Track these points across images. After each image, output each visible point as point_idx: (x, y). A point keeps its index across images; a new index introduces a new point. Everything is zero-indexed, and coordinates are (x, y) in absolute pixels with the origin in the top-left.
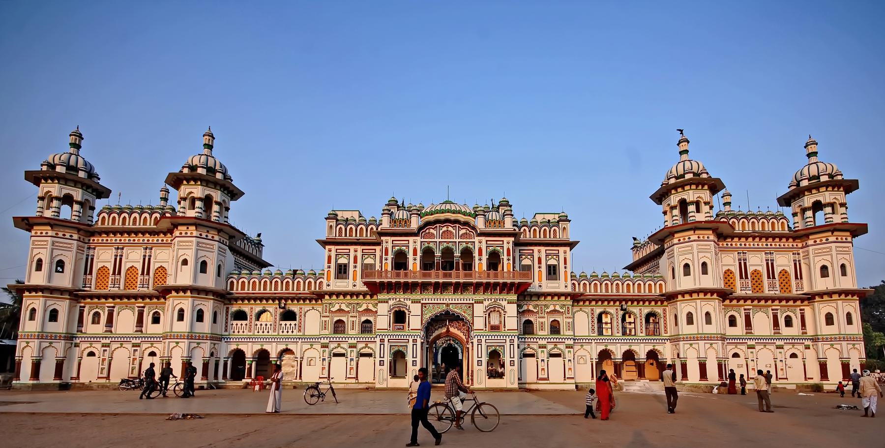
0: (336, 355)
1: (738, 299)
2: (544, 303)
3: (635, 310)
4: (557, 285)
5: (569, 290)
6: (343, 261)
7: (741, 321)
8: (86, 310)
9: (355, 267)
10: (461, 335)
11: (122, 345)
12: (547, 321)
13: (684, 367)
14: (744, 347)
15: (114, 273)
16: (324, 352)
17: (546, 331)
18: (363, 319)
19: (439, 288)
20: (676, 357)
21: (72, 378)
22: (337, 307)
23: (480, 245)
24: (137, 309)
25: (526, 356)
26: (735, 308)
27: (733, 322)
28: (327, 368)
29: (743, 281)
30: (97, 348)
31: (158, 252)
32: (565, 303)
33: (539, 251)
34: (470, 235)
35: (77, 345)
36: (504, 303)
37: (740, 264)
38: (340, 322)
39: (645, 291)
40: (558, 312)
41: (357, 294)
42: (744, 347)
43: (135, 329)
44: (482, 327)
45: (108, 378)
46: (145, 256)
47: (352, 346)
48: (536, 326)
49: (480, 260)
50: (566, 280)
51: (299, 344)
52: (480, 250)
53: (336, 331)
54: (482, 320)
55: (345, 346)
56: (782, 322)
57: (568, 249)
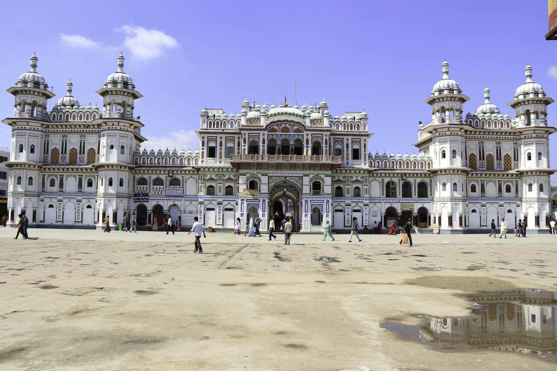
0: (209, 209)
2: (350, 175)
3: (411, 180)
6: (212, 144)
7: (478, 189)
8: (46, 177)
9: (221, 149)
10: (293, 196)
11: (70, 200)
14: (479, 205)
15: (62, 153)
16: (201, 206)
18: (227, 185)
19: (279, 166)
21: (41, 221)
22: (209, 177)
23: (307, 136)
24: (78, 177)
25: (337, 211)
27: (473, 189)
28: (203, 218)
29: (481, 161)
30: (54, 202)
31: (89, 138)
32: (364, 175)
33: (347, 139)
34: (301, 130)
35: (42, 201)
36: (323, 176)
37: (480, 149)
38: (211, 187)
40: (359, 181)
41: (222, 168)
42: (479, 205)
43: (77, 190)
44: (308, 192)
45: (63, 222)
46: (81, 141)
47: (220, 204)
48: (345, 191)
49: (307, 147)
50: (365, 160)
51: (183, 201)
52: (307, 140)
53: (208, 193)
55: (215, 203)
56: (504, 189)
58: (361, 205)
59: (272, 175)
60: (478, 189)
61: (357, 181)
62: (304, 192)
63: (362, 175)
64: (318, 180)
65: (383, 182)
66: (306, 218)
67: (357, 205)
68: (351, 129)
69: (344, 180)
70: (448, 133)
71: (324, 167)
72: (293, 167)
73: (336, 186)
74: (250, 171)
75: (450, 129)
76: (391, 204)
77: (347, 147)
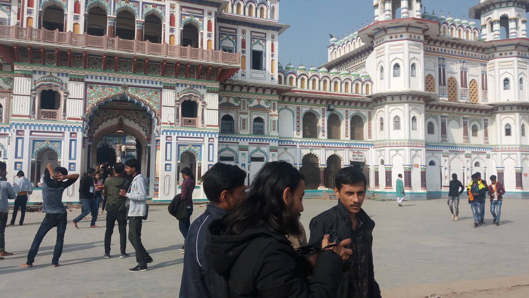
1: (437, 106)
2: (247, 96)
3: (341, 111)
4: (261, 76)
5: (275, 83)
12: (249, 118)
13: (388, 174)
17: (247, 132)
19: (111, 63)
20: (379, 163)
26: (434, 114)
32: (271, 98)
33: (244, 32)
37: (440, 69)
39: (351, 91)
48: (238, 124)
54: (173, 111)
57: (276, 33)
58: (265, 149)
59: (94, 80)
60: (437, 129)
61: (259, 108)
62: (164, 119)
63: (267, 98)
64: (193, 99)
65: (298, 113)
66: (167, 173)
67: (258, 150)
68: (250, 14)
69: (236, 104)
70: (405, 36)
71: (205, 72)
72: (143, 66)
73: (223, 114)
74: (42, 69)
75: (410, 29)
76: (311, 150)
77: (244, 46)
